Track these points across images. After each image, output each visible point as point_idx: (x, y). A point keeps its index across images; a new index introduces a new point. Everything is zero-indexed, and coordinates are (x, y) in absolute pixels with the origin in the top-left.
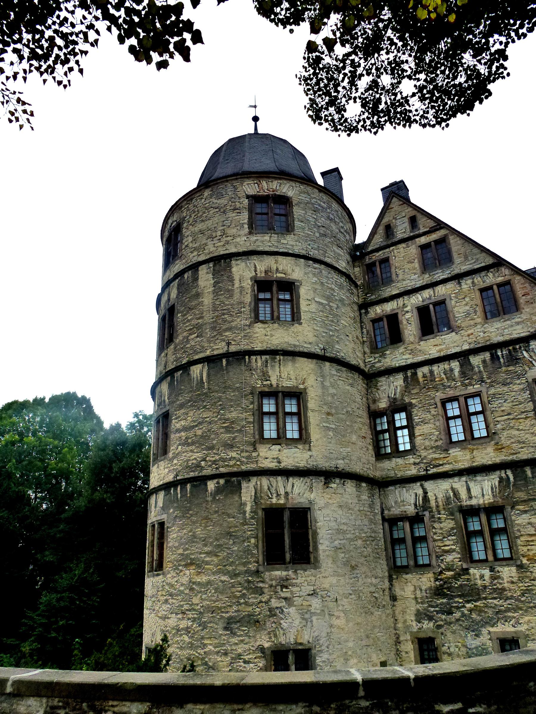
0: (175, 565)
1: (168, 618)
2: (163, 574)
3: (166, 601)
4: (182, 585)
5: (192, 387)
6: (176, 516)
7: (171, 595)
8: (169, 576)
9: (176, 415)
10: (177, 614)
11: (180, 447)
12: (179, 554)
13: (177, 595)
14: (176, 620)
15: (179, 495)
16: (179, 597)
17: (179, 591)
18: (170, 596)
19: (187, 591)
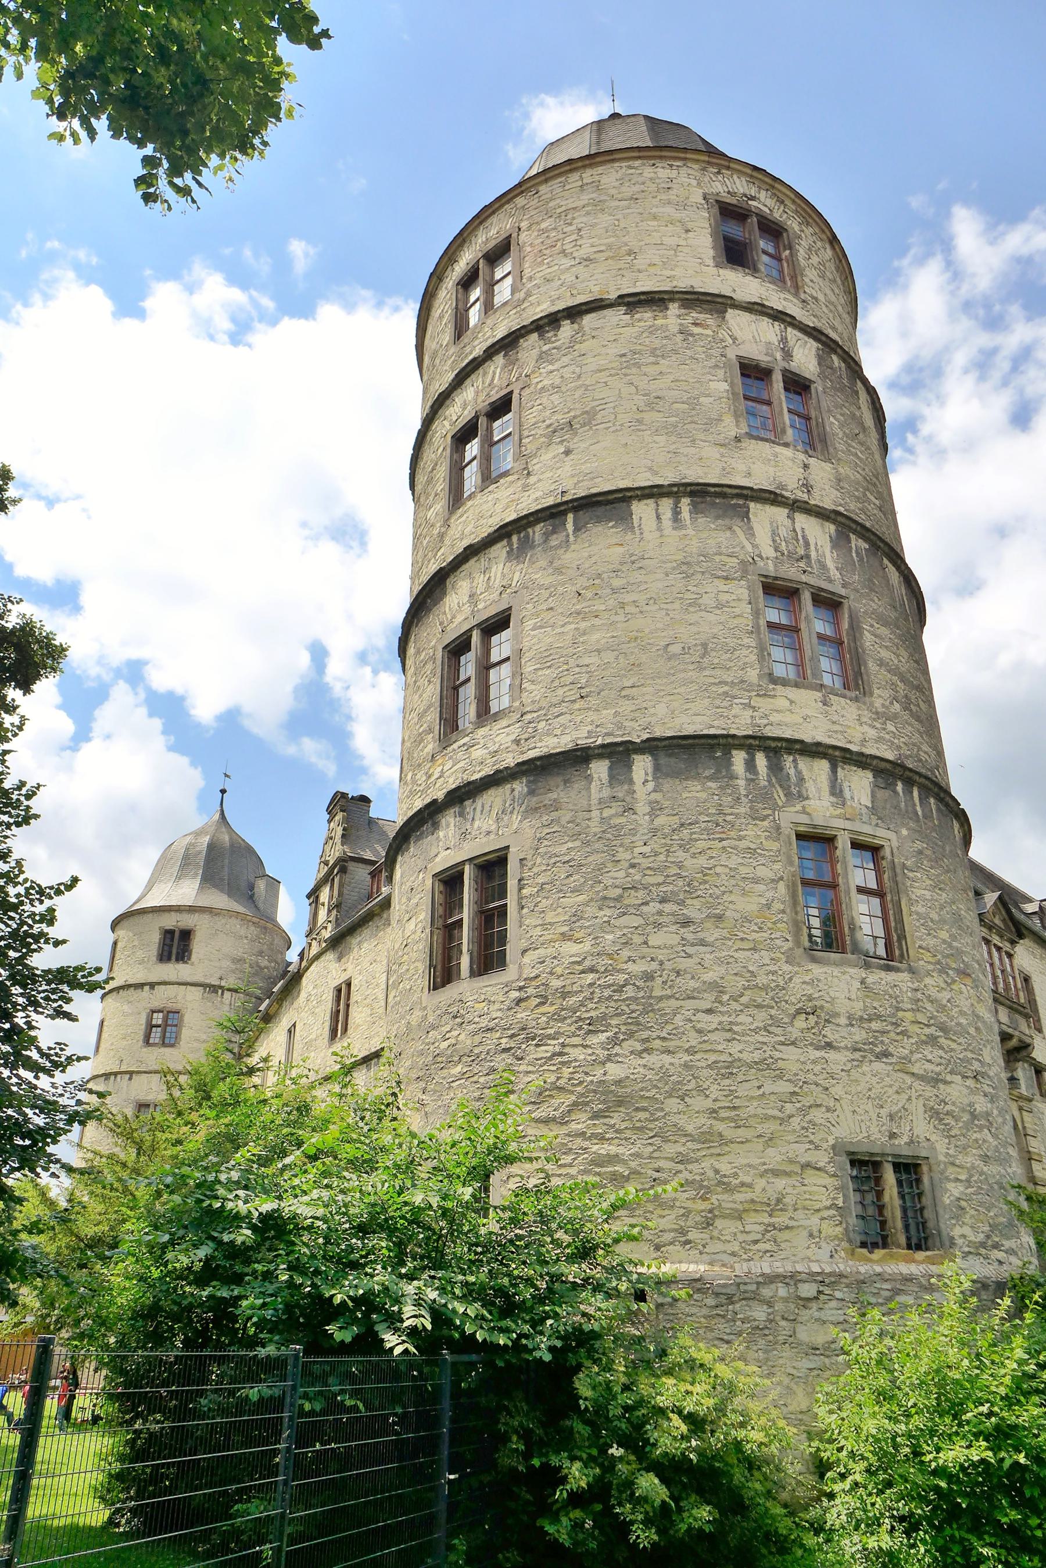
0: (939, 962)
1: (946, 1082)
2: (911, 971)
3: (932, 1040)
4: (962, 1013)
5: (894, 600)
6: (920, 852)
7: (943, 1028)
8: (928, 981)
9: (872, 626)
10: (965, 1077)
11: (897, 706)
12: (944, 941)
13: (955, 1034)
14: (965, 1091)
15: (918, 808)
16: (961, 1040)
17: (958, 1024)
18: (941, 1029)
19: (972, 1031)
